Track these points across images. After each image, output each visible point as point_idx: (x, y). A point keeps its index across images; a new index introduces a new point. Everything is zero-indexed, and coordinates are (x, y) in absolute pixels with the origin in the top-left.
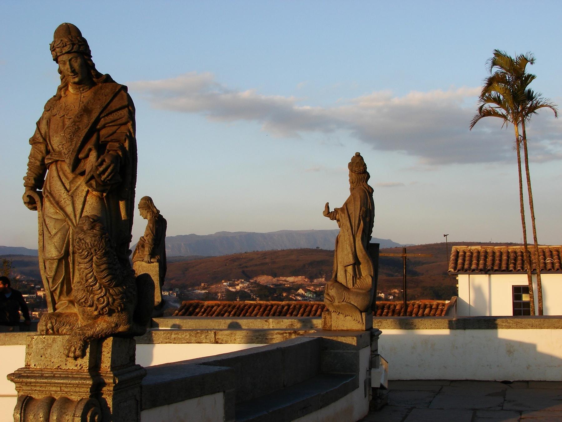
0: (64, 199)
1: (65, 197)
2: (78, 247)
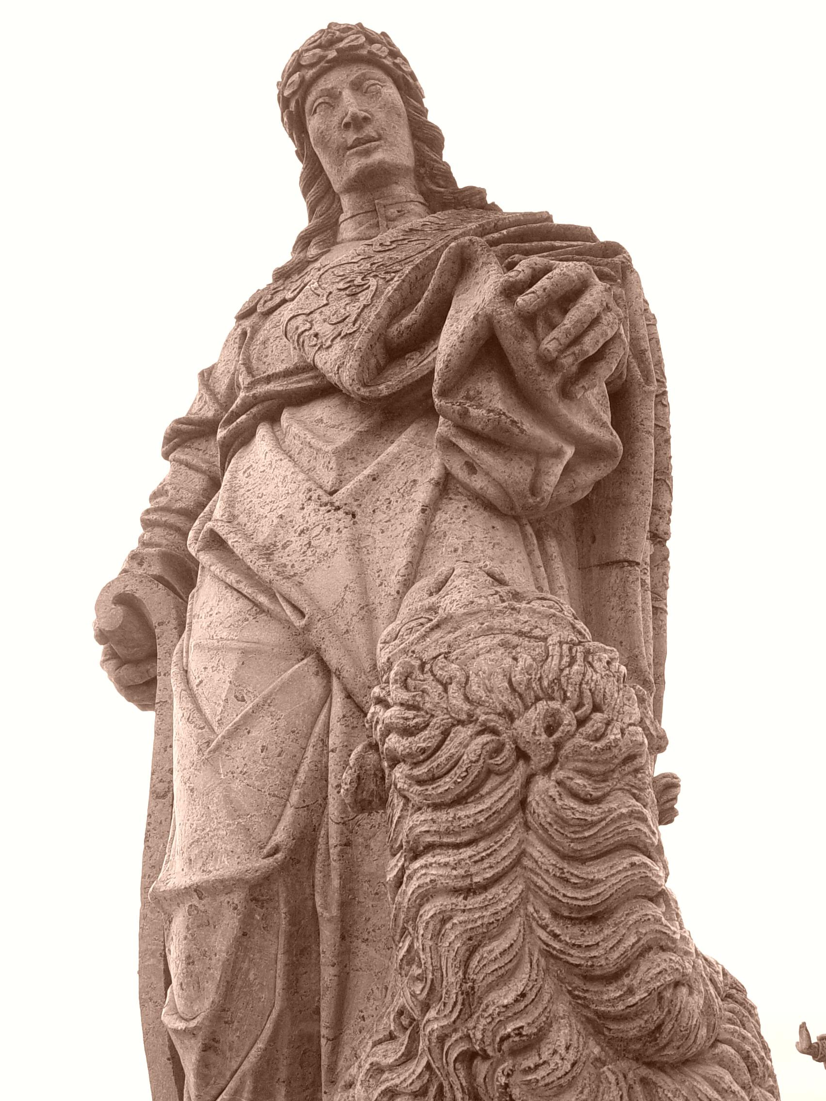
0: (302, 532)
1: (313, 519)
2: (410, 714)
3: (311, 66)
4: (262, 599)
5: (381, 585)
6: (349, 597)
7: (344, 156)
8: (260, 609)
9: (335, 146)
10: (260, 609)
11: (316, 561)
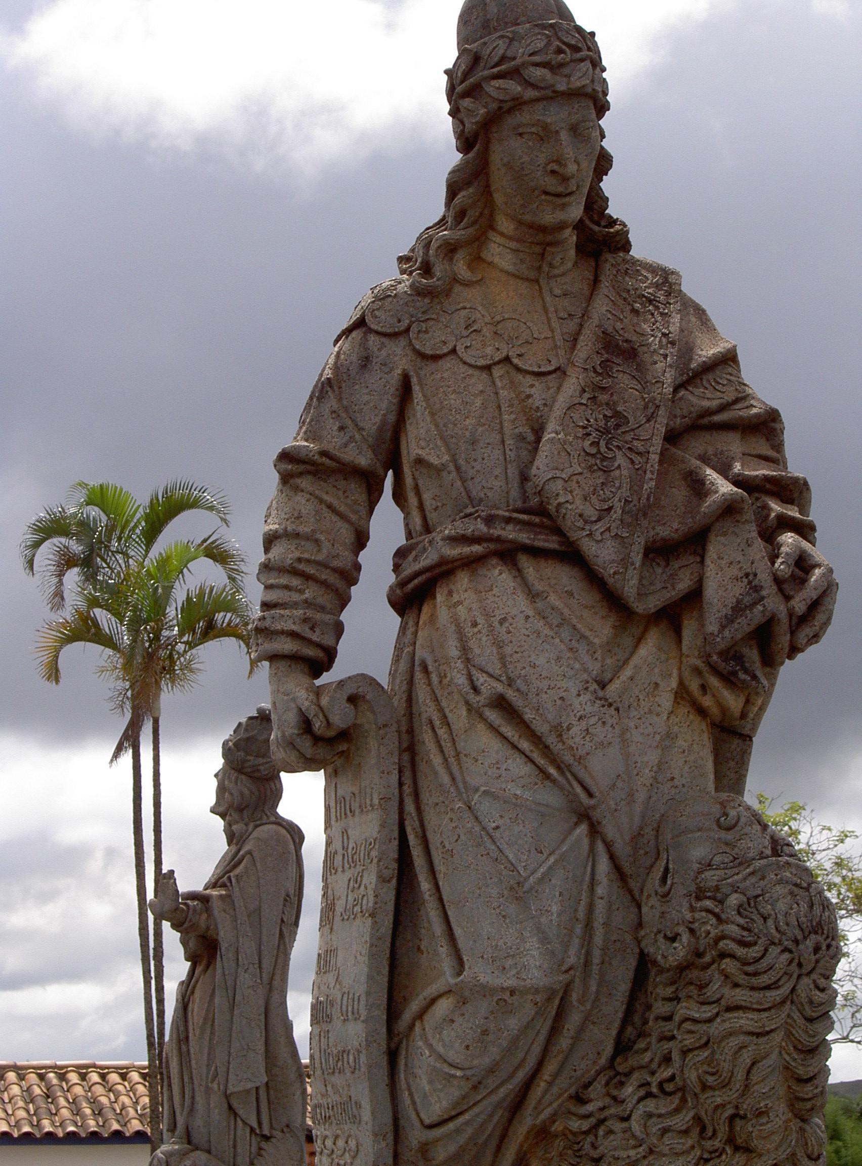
0: (581, 718)
1: (589, 708)
2: (745, 933)
3: (533, 86)
4: (552, 771)
5: (637, 775)
6: (620, 784)
7: (537, 198)
8: (547, 776)
9: (532, 184)
10: (547, 776)
11: (594, 747)
